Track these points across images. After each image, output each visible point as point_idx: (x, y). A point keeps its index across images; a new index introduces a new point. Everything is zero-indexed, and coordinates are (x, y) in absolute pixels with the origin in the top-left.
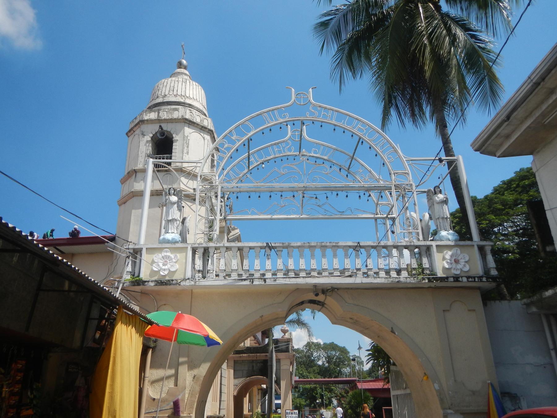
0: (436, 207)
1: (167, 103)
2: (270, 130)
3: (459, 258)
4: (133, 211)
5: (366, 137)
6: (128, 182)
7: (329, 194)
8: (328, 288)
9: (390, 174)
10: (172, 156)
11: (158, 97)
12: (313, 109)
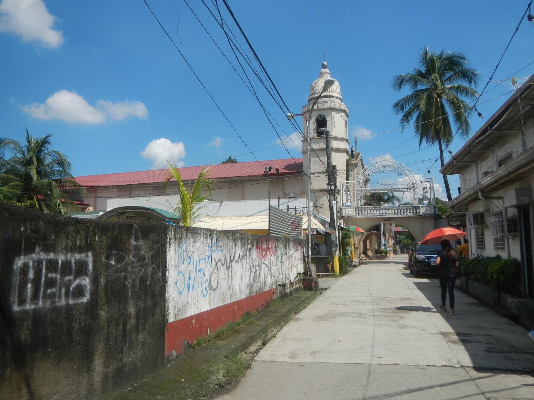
11: (315, 93)
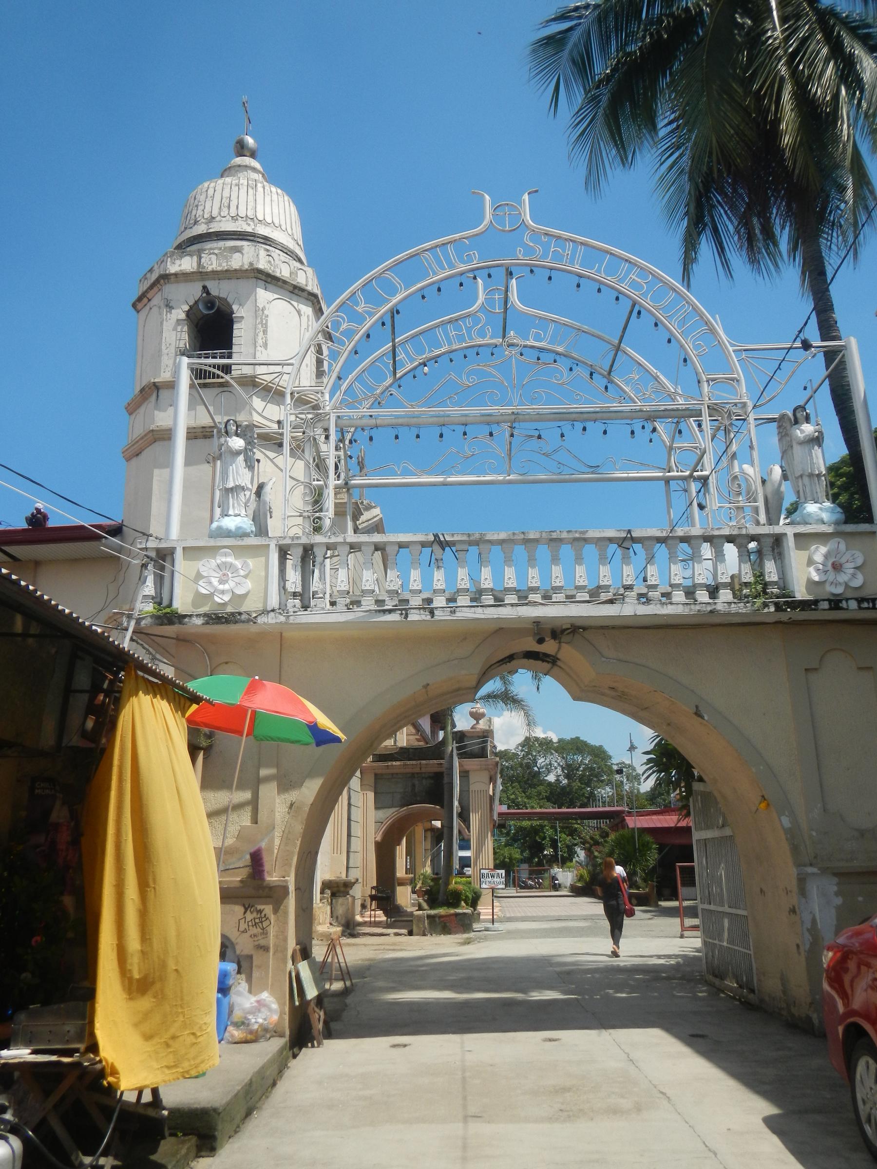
0: (798, 451)
1: (217, 236)
2: (439, 290)
3: (843, 560)
4: (156, 472)
5: (648, 301)
6: (142, 410)
7: (566, 427)
8: (564, 627)
9: (699, 382)
10: (231, 353)
11: (196, 222)
12: (531, 241)
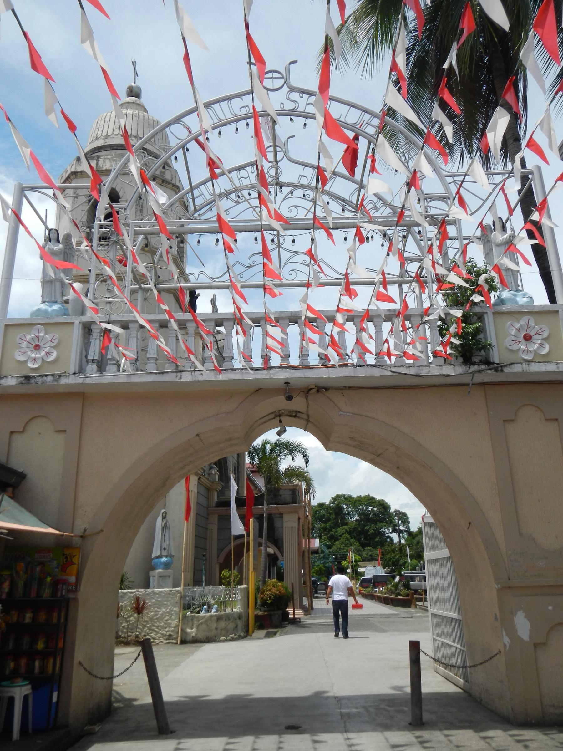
3: (532, 334)
